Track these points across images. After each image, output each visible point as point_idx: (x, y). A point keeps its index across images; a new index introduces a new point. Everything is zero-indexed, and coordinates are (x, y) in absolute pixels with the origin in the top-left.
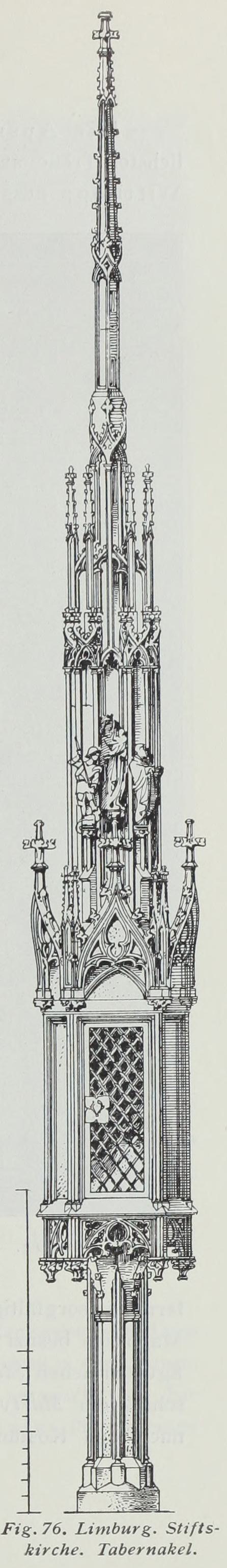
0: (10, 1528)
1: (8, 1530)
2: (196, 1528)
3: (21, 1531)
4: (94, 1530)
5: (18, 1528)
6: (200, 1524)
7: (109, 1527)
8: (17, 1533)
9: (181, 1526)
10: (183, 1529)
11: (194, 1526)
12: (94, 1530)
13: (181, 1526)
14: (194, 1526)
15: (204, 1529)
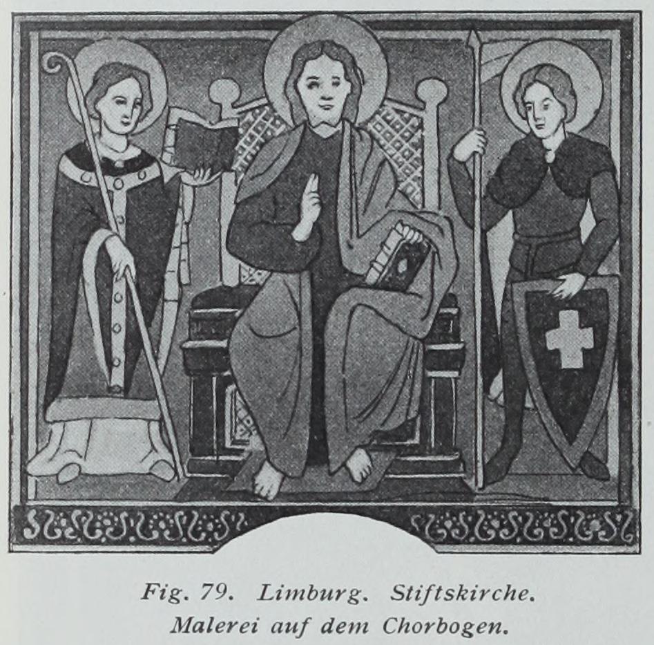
0: (153, 592)
1: (150, 593)
2: (431, 592)
3: (168, 594)
4: (284, 595)
5: (164, 591)
6: (438, 587)
7: (303, 591)
8: (162, 598)
9: (411, 589)
10: (413, 594)
11: (429, 590)
12: (284, 595)
13: (411, 589)
14: (429, 590)
15: (443, 594)
